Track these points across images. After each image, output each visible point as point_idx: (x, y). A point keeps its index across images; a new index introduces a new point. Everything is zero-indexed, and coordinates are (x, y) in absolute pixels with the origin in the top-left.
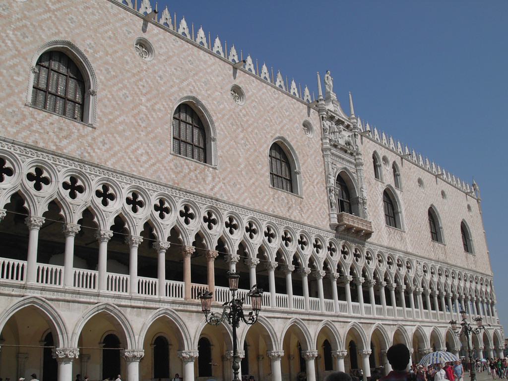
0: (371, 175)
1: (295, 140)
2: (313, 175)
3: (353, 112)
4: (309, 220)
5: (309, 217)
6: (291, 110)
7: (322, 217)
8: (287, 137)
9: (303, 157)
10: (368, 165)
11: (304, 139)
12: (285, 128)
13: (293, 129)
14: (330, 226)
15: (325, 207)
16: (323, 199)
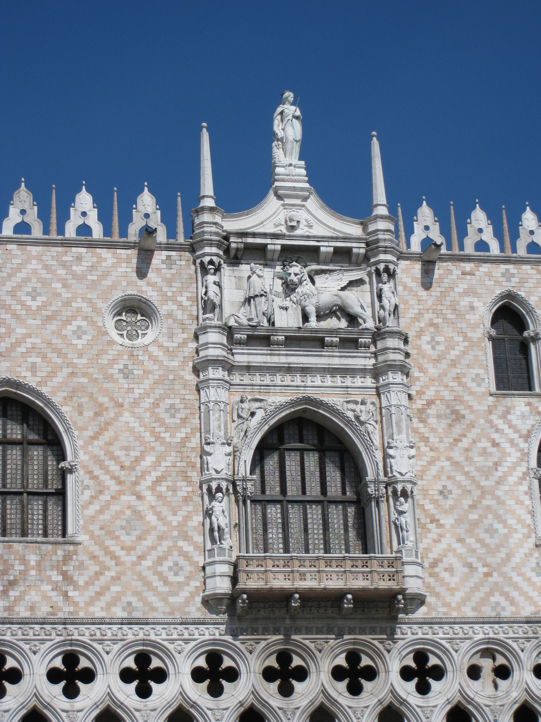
0: (473, 385)
1: (66, 371)
2: (137, 460)
3: (380, 194)
4: (103, 604)
5: (99, 594)
6: (57, 286)
7: (166, 582)
8: (29, 374)
9: (97, 414)
10: (453, 354)
11: (104, 361)
12: (22, 349)
13: (54, 341)
14: (206, 602)
15: (190, 549)
16: (182, 525)
